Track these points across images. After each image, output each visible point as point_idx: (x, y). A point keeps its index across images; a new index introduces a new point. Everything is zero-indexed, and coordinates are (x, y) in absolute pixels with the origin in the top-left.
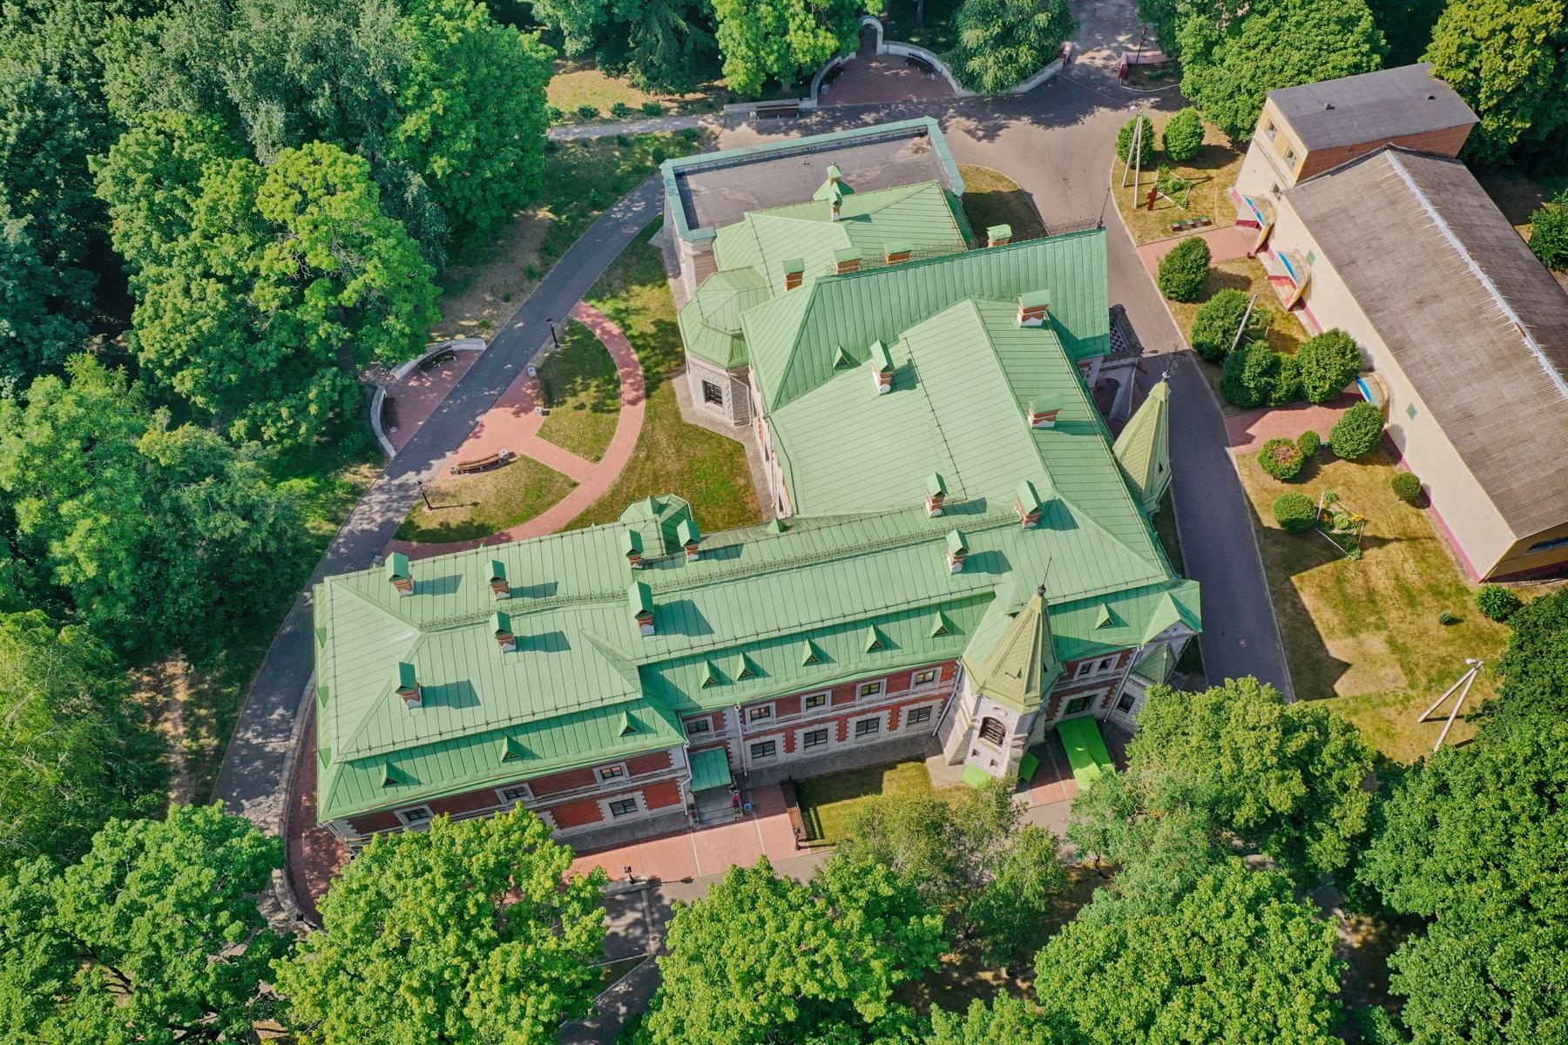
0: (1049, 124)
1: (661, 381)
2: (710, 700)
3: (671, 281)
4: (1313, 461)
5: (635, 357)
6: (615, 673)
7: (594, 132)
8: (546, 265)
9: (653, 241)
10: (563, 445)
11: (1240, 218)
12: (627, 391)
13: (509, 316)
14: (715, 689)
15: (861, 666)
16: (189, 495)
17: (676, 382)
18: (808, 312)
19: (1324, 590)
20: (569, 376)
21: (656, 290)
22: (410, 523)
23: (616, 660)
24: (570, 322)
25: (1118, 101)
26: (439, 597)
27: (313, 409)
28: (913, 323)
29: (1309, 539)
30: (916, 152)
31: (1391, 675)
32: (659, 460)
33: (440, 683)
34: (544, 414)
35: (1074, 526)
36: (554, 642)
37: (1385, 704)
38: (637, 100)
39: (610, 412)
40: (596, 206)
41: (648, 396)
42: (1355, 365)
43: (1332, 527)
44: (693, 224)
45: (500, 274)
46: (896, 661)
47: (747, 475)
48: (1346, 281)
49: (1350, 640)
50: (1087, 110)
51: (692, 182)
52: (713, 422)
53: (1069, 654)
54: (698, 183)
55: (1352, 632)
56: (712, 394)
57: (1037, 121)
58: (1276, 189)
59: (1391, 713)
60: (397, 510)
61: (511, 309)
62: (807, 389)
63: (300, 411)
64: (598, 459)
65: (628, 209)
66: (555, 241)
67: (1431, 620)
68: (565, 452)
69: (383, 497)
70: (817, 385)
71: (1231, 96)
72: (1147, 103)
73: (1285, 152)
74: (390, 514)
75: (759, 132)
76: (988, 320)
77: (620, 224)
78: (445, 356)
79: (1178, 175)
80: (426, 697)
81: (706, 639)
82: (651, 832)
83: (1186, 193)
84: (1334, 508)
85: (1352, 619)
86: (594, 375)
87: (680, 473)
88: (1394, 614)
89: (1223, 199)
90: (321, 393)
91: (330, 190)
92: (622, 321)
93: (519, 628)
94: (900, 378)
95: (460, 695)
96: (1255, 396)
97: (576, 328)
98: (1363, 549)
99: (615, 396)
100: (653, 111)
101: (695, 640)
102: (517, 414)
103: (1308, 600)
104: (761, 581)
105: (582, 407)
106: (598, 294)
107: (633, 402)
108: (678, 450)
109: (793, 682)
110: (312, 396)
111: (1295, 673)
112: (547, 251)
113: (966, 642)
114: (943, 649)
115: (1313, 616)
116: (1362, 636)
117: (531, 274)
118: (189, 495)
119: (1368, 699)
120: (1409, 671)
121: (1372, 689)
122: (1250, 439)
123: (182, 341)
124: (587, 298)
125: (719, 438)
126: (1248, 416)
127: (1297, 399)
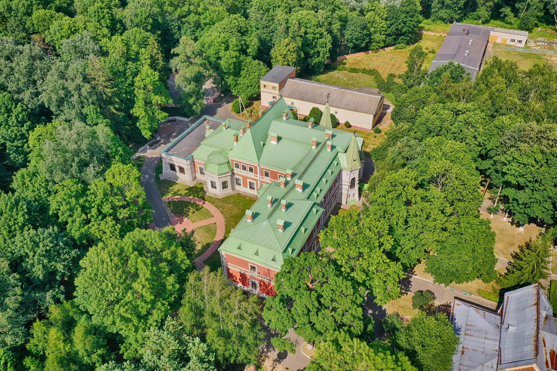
5: (191, 197)
12: (201, 203)
47: (247, 196)
64: (213, 216)
68: (204, 221)
72: (225, 104)
75: (154, 149)
81: (310, 187)
102: (181, 223)
125: (230, 197)
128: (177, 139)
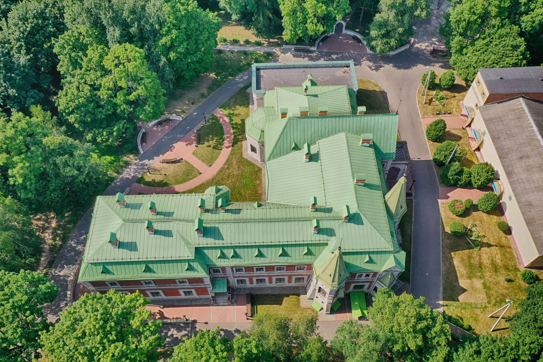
0: (399, 68)
1: (239, 141)
2: (220, 263)
3: (250, 106)
4: (469, 210)
5: (232, 131)
6: (186, 248)
7: (236, 48)
8: (209, 93)
9: (248, 91)
10: (200, 159)
11: (462, 113)
12: (226, 143)
13: (192, 110)
14: (222, 260)
15: (275, 261)
16: (59, 160)
17: (244, 142)
18: (284, 128)
19: (463, 259)
20: (207, 135)
21: (245, 109)
22: (142, 178)
23: (187, 243)
24: (213, 115)
25: (427, 63)
26: (133, 210)
27: (115, 134)
28: (322, 138)
29: (462, 239)
30: (344, 73)
31: (481, 298)
32: (232, 169)
33: (126, 241)
34: (196, 146)
35: (362, 224)
36: (168, 234)
37: (477, 308)
38: (254, 39)
39: (219, 149)
40: (231, 75)
41: (233, 146)
42: (492, 176)
43: (471, 236)
44: (258, 88)
45: (192, 95)
46: (289, 261)
47: (260, 180)
48: (495, 145)
49: (469, 281)
50: (415, 65)
51: (262, 72)
52: (253, 158)
53: (353, 270)
54: (264, 73)
55: (470, 278)
56: (253, 149)
57: (395, 66)
58: (477, 105)
59: (478, 311)
60: (139, 173)
61: (194, 107)
62: (281, 155)
63: (110, 134)
64: (211, 165)
65: (242, 78)
66: (215, 85)
67: (502, 279)
68: (200, 161)
69: (136, 167)
70: (284, 154)
71: (467, 68)
72: (438, 65)
73: (481, 92)
74: (136, 173)
75: (294, 56)
76: (349, 141)
77: (238, 83)
78: (168, 120)
79: (443, 93)
80: (121, 245)
81: (221, 242)
82: (198, 303)
83: (444, 101)
84: (474, 229)
85: (471, 272)
86: (217, 136)
87: (238, 175)
88: (488, 274)
89: (458, 105)
90: (118, 129)
91: (129, 61)
92: (230, 117)
93: (156, 226)
94: (312, 158)
95: (132, 246)
96: (452, 182)
97: (214, 118)
98: (481, 247)
99: (222, 144)
100: (259, 44)
101: (217, 241)
102: (187, 145)
103: (456, 262)
104: (244, 224)
105: (209, 146)
106: (224, 107)
107: (227, 148)
108: (239, 167)
109: (250, 262)
110: (115, 129)
111: (445, 289)
112: (210, 89)
113: (315, 259)
114: (307, 260)
115: (457, 269)
116: (474, 280)
117: (203, 96)
118: (59, 160)
119: (470, 304)
120: (489, 297)
121: (473, 301)
122: (448, 197)
123: (73, 105)
124: (220, 108)
125: (254, 165)
126: (449, 188)
127: (468, 185)
128: (311, 63)
